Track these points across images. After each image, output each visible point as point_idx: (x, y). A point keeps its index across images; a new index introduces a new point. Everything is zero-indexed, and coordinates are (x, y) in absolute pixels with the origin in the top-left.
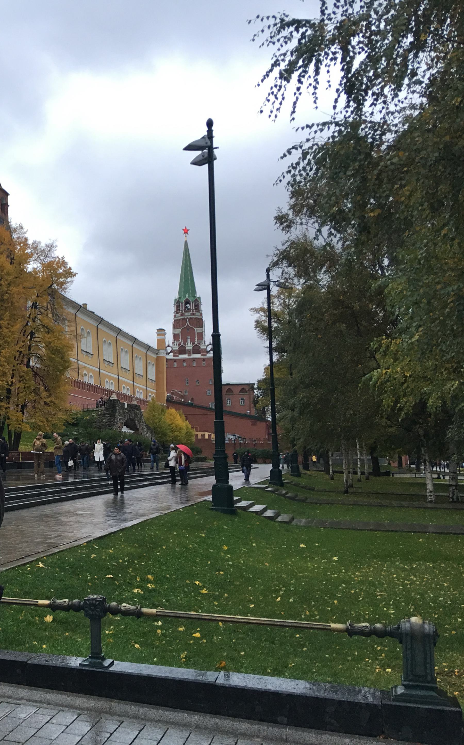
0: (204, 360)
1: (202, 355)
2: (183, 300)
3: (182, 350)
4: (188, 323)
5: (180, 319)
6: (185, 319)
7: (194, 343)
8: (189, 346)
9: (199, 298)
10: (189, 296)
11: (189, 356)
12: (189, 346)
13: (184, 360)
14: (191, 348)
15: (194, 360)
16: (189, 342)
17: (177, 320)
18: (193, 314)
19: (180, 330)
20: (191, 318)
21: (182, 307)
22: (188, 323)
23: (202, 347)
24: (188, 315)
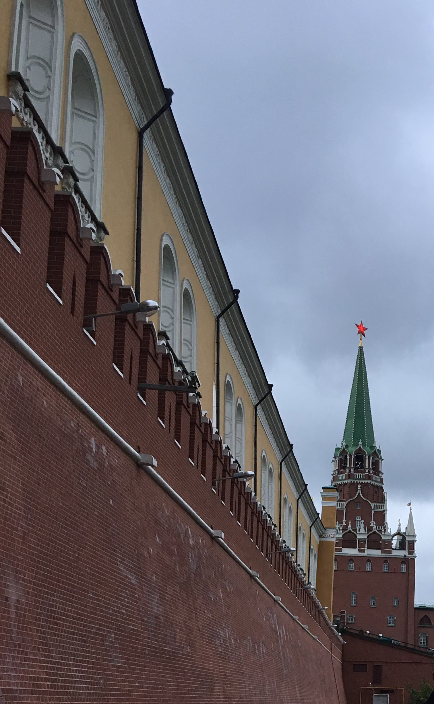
0: (386, 560)
2: (352, 450)
3: (348, 541)
5: (345, 484)
6: (355, 485)
7: (370, 529)
8: (362, 534)
10: (364, 445)
11: (360, 551)
12: (362, 534)
13: (351, 559)
14: (366, 537)
15: (369, 559)
16: (362, 526)
17: (340, 485)
18: (370, 478)
19: (345, 504)
20: (366, 484)
21: (351, 462)
23: (383, 538)
24: (360, 478)
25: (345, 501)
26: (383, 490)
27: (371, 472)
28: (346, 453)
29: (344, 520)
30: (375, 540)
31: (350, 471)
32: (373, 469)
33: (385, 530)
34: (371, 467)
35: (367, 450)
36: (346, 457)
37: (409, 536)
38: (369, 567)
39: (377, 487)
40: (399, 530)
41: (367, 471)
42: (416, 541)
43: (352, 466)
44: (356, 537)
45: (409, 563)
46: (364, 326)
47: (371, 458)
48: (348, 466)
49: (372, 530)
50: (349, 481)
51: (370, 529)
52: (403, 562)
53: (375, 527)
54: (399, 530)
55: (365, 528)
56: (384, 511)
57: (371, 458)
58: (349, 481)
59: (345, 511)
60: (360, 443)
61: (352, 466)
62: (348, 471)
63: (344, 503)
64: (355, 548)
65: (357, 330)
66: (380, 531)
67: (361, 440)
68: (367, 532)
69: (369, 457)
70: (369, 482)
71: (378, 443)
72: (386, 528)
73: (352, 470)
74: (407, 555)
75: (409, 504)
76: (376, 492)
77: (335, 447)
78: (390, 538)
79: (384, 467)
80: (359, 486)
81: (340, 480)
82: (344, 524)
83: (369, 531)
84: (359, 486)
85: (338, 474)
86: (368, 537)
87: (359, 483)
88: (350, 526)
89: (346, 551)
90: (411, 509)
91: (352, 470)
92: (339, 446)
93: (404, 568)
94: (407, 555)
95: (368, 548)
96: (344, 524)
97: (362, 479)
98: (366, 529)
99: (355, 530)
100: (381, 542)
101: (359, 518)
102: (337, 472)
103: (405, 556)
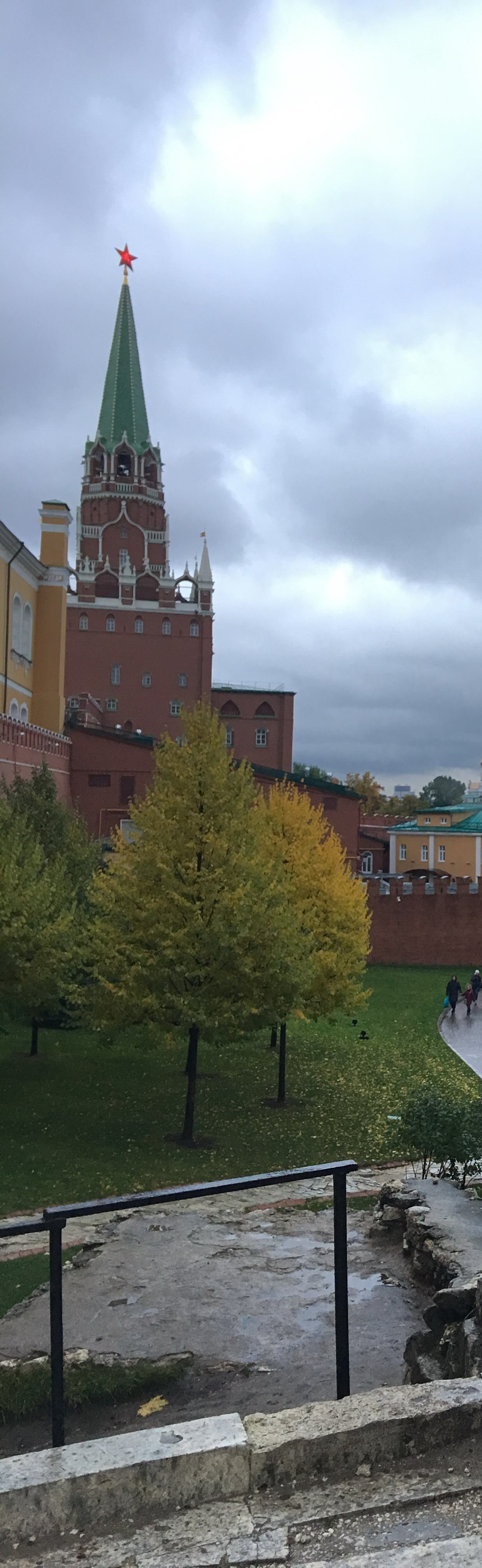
0: (166, 618)
1: (161, 605)
3: (106, 586)
4: (124, 511)
5: (101, 500)
8: (127, 577)
9: (157, 451)
10: (131, 440)
12: (127, 577)
13: (111, 614)
14: (134, 581)
15: (139, 615)
16: (128, 564)
17: (93, 500)
18: (140, 491)
19: (101, 529)
20: (136, 501)
21: (110, 465)
22: (124, 511)
23: (162, 584)
24: (124, 492)
25: (101, 525)
26: (164, 511)
27: (143, 481)
28: (103, 450)
29: (100, 554)
30: (149, 588)
31: (109, 479)
32: (146, 477)
33: (164, 573)
34: (142, 475)
35: (135, 449)
36: (102, 458)
37: (202, 582)
38: (139, 627)
39: (154, 505)
40: (187, 572)
41: (136, 480)
42: (213, 591)
43: (112, 471)
44: (118, 580)
45: (203, 621)
46: (132, 252)
47: (143, 461)
48: (105, 471)
49: (143, 571)
50: (108, 495)
51: (141, 570)
52: (193, 621)
53: (147, 567)
54: (187, 572)
55: (131, 568)
56: (164, 543)
57: (143, 461)
58: (108, 495)
59: (100, 540)
60: (125, 436)
61: (112, 471)
62: (105, 478)
63: (100, 528)
64: (117, 597)
65: (119, 258)
66: (157, 573)
67: (125, 432)
68: (134, 575)
69: (140, 458)
70: (140, 497)
71: (156, 438)
72: (166, 570)
73: (112, 478)
74: (199, 610)
75: (203, 535)
76: (152, 514)
77: (85, 441)
78: (172, 584)
79: (165, 476)
80: (124, 503)
81: (92, 493)
82: (100, 560)
83: (138, 572)
84: (124, 503)
85: (91, 482)
86: (137, 581)
87: (124, 499)
88: (107, 564)
89: (103, 603)
90: (205, 542)
91: (112, 478)
92: (93, 439)
93: (195, 631)
94: (199, 610)
95: (137, 598)
96: (100, 560)
97: (128, 493)
98: (134, 569)
99: (117, 571)
100: (157, 590)
101: (124, 553)
102: (88, 480)
103: (197, 612)
